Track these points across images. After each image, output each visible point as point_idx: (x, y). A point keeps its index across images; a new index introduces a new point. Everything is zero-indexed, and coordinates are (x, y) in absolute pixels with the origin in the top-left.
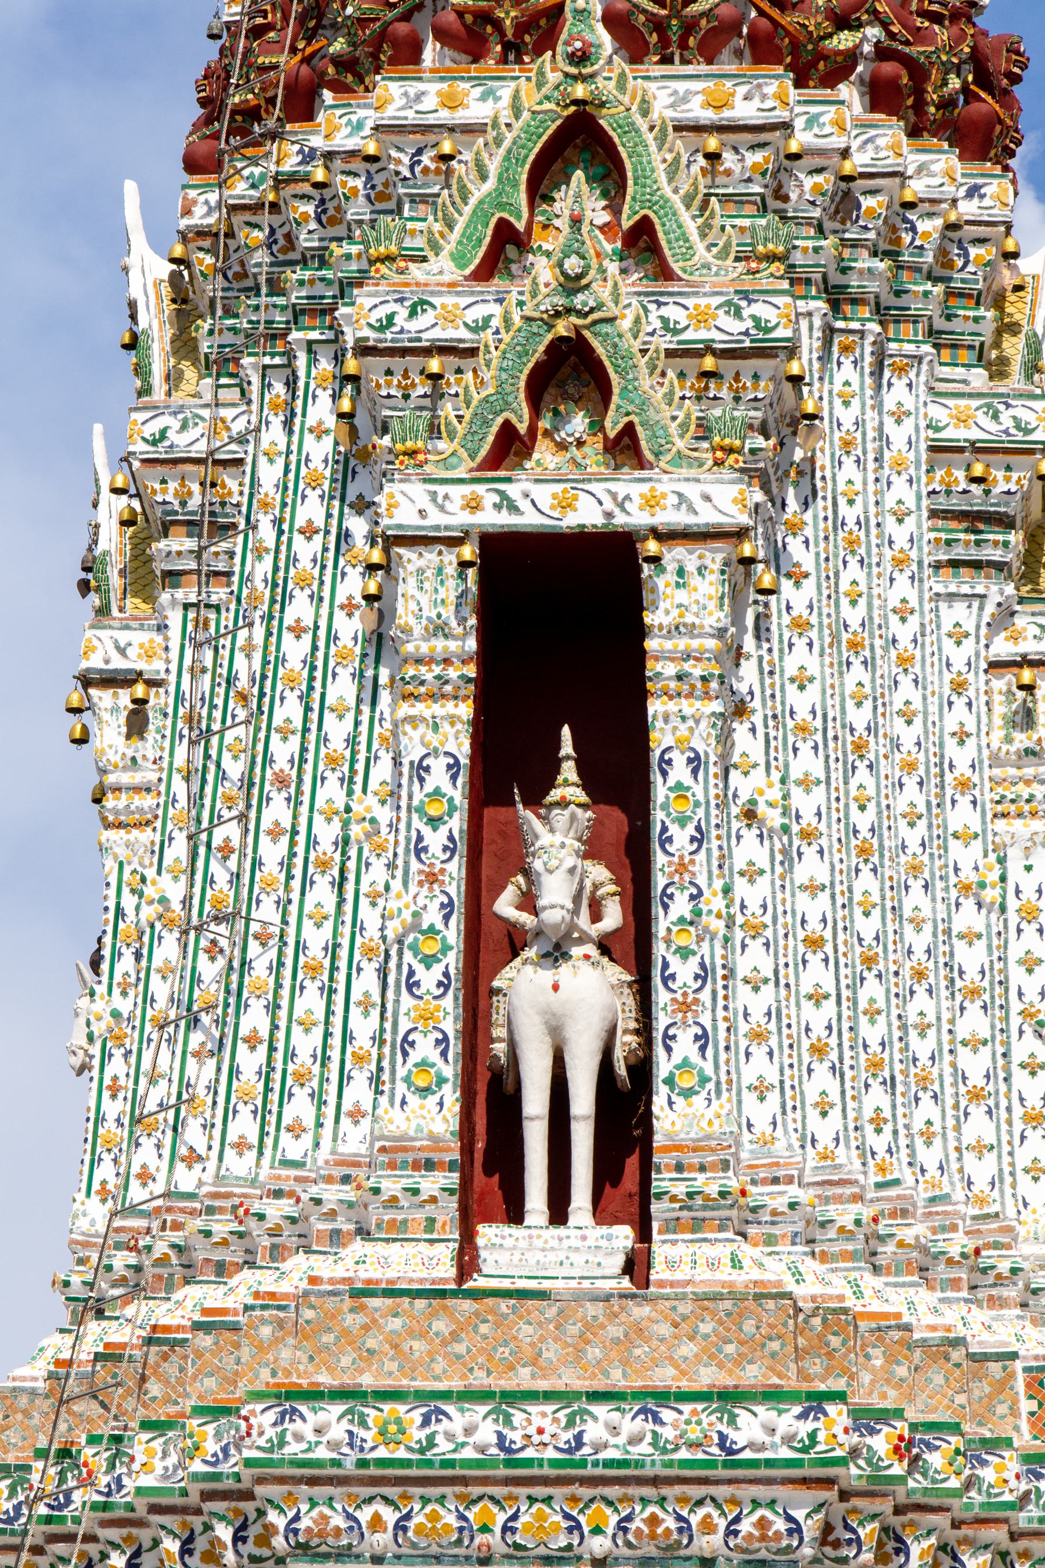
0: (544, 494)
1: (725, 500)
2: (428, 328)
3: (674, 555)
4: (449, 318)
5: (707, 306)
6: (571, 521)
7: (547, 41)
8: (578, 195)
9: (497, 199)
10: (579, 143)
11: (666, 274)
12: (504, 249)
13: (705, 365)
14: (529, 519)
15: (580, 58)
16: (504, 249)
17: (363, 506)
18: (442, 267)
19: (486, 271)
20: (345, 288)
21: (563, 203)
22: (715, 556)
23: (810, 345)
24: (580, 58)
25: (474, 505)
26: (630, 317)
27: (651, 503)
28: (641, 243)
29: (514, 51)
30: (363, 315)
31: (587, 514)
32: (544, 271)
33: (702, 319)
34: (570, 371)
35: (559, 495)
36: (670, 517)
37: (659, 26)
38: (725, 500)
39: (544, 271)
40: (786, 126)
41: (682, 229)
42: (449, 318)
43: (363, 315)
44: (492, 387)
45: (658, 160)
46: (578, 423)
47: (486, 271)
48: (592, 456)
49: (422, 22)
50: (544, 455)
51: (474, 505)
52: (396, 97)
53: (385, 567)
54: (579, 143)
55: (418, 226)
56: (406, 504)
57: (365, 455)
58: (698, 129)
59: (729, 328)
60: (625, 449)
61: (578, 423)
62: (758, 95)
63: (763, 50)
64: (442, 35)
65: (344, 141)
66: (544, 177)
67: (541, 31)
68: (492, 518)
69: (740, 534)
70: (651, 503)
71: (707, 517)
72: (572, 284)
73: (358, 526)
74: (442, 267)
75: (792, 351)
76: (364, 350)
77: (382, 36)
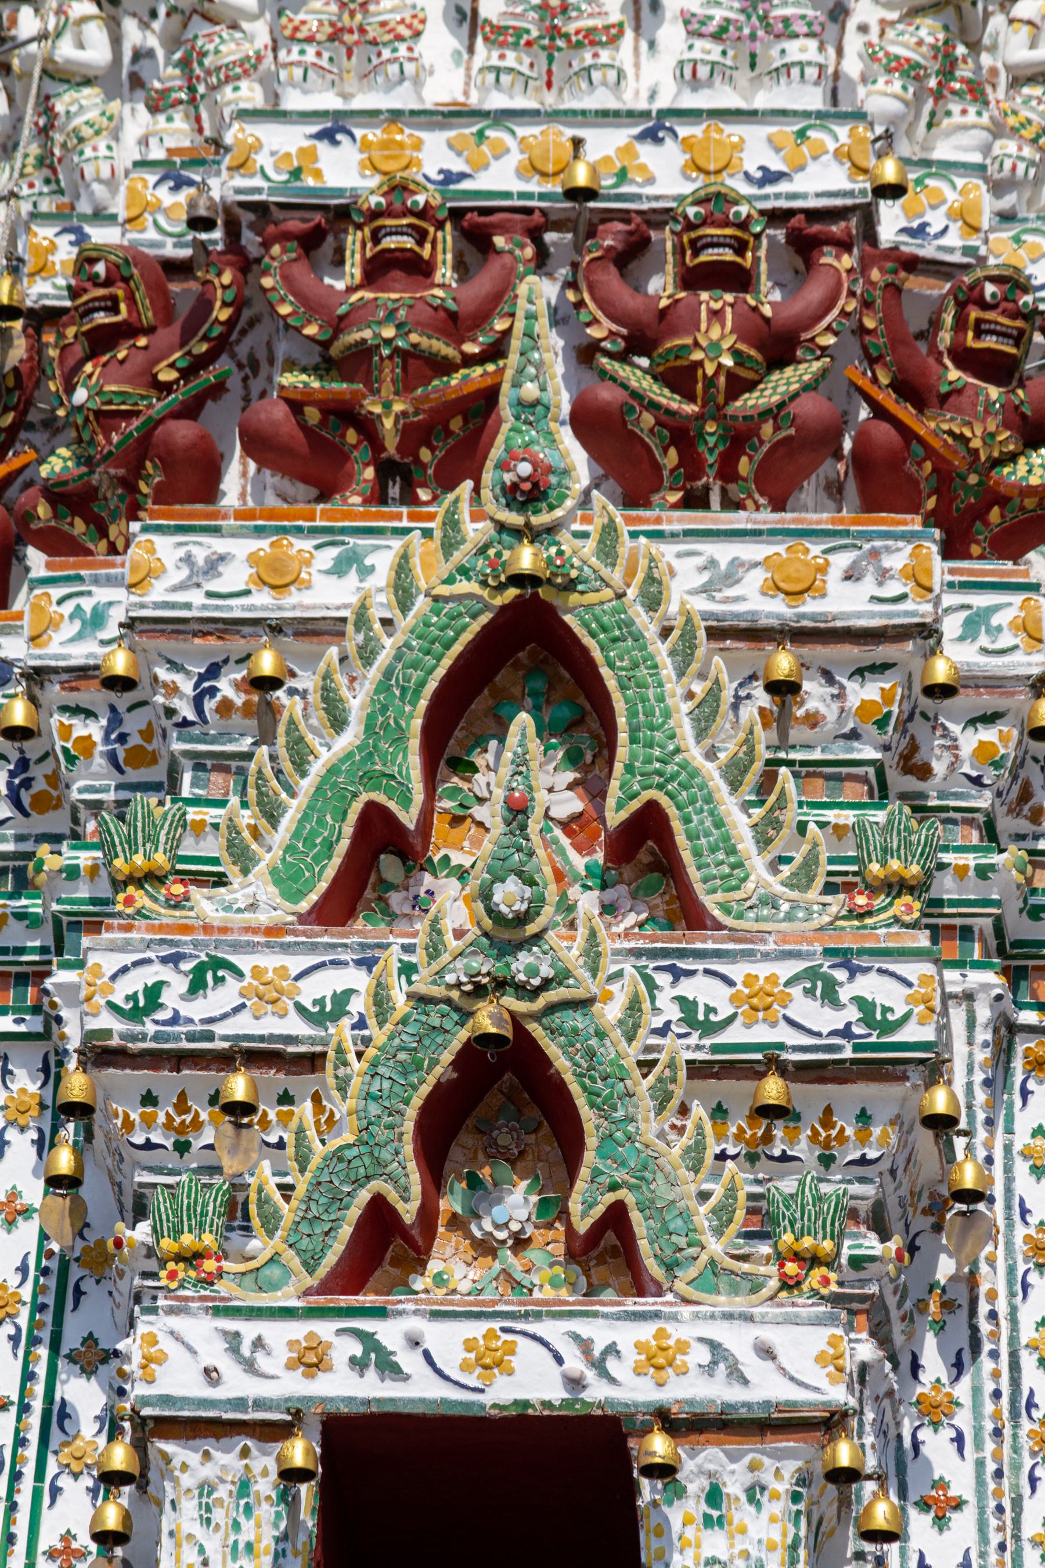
0: (449, 1341)
1: (800, 1357)
2: (223, 1012)
3: (702, 1462)
4: (268, 995)
5: (765, 984)
6: (501, 1393)
7: (463, 461)
8: (522, 760)
9: (363, 766)
10: (525, 658)
11: (690, 915)
12: (377, 862)
13: (763, 1092)
14: (419, 1389)
15: (529, 494)
16: (377, 862)
17: (94, 1358)
18: (256, 896)
19: (340, 906)
20: (65, 933)
21: (492, 776)
22: (781, 1466)
23: (968, 1057)
24: (529, 494)
25: (311, 1360)
26: (621, 997)
27: (658, 1361)
28: (644, 854)
29: (398, 480)
30: (102, 984)
31: (532, 1382)
32: (453, 907)
33: (760, 1003)
34: (501, 1100)
35: (478, 1344)
36: (694, 1388)
37: (681, 434)
38: (800, 1357)
39: (453, 907)
40: (927, 633)
41: (723, 827)
42: (268, 995)
43: (102, 984)
44: (351, 1128)
45: (677, 697)
46: (517, 1204)
47: (340, 906)
48: (544, 1268)
49: (222, 422)
50: (450, 1264)
51: (311, 1360)
52: (169, 564)
53: (137, 1479)
54: (525, 658)
55: (208, 816)
56: (181, 1355)
57: (100, 1259)
58: (755, 634)
59: (815, 1022)
60: (608, 1255)
61: (517, 1204)
62: (870, 572)
63: (882, 483)
64: (260, 446)
65: (67, 647)
66: (456, 721)
67: (453, 440)
68: (344, 1386)
69: (832, 1423)
70: (658, 1361)
71: (767, 1388)
72: (509, 932)
73: (86, 1396)
74: (256, 896)
75: (934, 1068)
76: (100, 1054)
77: (143, 447)
